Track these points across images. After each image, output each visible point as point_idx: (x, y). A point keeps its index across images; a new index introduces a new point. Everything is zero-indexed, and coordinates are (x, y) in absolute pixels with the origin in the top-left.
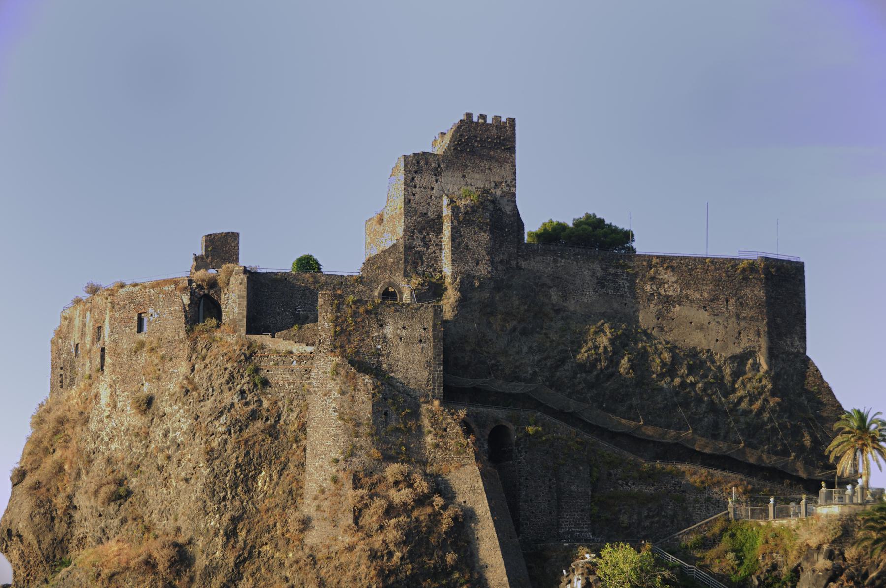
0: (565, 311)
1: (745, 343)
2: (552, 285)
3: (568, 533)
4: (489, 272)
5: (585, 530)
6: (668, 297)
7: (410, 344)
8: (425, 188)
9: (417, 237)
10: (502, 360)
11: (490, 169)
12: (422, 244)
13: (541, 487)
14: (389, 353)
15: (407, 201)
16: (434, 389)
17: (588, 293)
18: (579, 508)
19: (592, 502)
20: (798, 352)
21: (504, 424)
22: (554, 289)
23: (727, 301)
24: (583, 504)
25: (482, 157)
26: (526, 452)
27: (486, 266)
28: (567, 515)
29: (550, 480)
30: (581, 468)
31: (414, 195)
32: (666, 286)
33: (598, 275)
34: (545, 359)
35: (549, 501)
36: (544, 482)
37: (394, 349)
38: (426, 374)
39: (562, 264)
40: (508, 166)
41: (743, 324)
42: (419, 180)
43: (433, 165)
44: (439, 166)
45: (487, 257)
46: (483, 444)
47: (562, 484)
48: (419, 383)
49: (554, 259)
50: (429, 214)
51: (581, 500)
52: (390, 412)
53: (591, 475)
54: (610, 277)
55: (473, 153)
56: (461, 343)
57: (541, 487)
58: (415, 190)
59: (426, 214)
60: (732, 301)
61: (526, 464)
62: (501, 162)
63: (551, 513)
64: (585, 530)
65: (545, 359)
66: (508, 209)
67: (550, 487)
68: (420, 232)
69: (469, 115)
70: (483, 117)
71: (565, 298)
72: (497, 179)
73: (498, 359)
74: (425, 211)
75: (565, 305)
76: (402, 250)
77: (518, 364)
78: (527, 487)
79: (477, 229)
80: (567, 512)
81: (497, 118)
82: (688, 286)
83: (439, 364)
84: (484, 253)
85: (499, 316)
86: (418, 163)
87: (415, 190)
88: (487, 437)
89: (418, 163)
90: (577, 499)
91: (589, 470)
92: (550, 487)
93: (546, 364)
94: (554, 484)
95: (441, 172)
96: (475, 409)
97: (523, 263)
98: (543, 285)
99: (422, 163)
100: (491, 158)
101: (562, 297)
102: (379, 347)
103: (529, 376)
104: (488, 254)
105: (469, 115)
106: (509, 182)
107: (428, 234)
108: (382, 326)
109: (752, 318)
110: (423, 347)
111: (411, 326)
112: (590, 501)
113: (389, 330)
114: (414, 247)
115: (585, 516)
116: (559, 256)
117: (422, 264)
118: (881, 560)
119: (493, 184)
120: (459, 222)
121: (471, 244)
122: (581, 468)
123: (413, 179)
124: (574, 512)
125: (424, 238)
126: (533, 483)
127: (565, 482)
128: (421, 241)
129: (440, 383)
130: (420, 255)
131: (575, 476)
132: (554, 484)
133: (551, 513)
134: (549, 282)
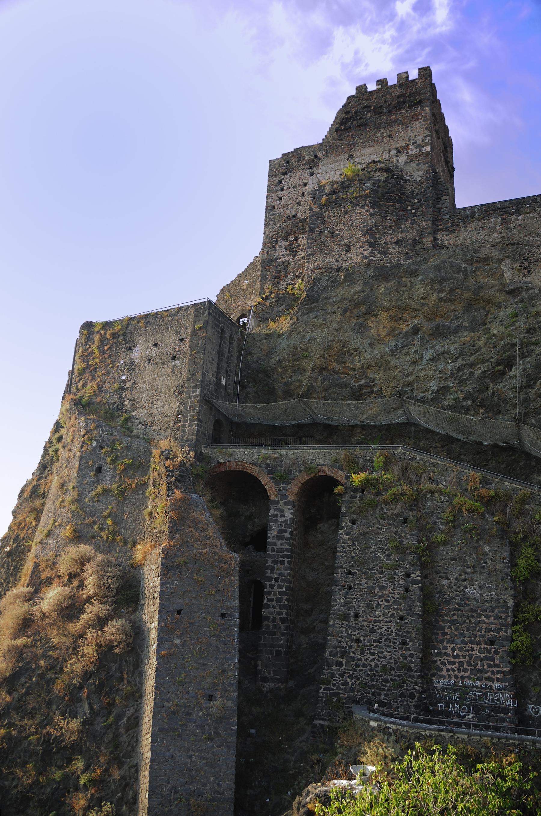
0: (527, 290)
2: (501, 257)
3: (455, 689)
4: (365, 258)
5: (496, 685)
7: (160, 365)
8: (294, 187)
9: (280, 246)
10: (378, 375)
11: (390, 136)
12: (288, 252)
13: (383, 588)
14: (134, 383)
15: (270, 209)
16: (184, 426)
18: (482, 636)
19: (514, 624)
21: (327, 474)
22: (508, 261)
24: (493, 627)
25: (378, 128)
26: (354, 522)
27: (361, 250)
28: (453, 650)
29: (408, 575)
30: (487, 549)
31: (280, 199)
34: (471, 365)
35: (401, 618)
36: (391, 579)
37: (140, 377)
38: (175, 405)
39: (519, 223)
42: (287, 181)
43: (307, 158)
44: (316, 156)
45: (363, 239)
46: (282, 511)
47: (445, 582)
48: (166, 419)
49: (503, 219)
50: (299, 215)
51: (487, 617)
52: (106, 467)
53: (513, 565)
56: (295, 360)
57: (383, 588)
58: (280, 194)
59: (294, 216)
61: (350, 543)
63: (404, 643)
64: (496, 685)
65: (471, 365)
67: (407, 590)
68: (286, 238)
70: (382, 82)
71: (527, 270)
72: (401, 144)
73: (371, 376)
74: (293, 213)
75: (528, 280)
76: (259, 267)
77: (410, 379)
78: (350, 588)
79: (349, 207)
80: (453, 642)
81: (403, 78)
83: (195, 387)
84: (360, 233)
85: (384, 315)
86: (288, 162)
87: (280, 194)
88: (291, 498)
89: (288, 162)
90: (480, 616)
91: (507, 554)
92: (407, 590)
93: (471, 374)
94: (414, 582)
95: (318, 163)
96: (270, 452)
97: (446, 238)
98: (486, 260)
99: (293, 160)
100: (390, 124)
101: (520, 270)
102: (124, 378)
103: (429, 395)
104: (364, 235)
107: (296, 239)
108: (130, 349)
110: (175, 366)
112: (510, 620)
114: (276, 259)
115: (496, 652)
116: (514, 213)
117: (286, 277)
119: (394, 152)
120: (321, 206)
122: (487, 549)
123: (280, 182)
124: (471, 642)
125: (291, 245)
126: (364, 581)
127: (452, 578)
128: (286, 249)
129: (193, 416)
130: (285, 266)
131: (474, 567)
132: (414, 582)
133: (404, 643)
134: (496, 254)
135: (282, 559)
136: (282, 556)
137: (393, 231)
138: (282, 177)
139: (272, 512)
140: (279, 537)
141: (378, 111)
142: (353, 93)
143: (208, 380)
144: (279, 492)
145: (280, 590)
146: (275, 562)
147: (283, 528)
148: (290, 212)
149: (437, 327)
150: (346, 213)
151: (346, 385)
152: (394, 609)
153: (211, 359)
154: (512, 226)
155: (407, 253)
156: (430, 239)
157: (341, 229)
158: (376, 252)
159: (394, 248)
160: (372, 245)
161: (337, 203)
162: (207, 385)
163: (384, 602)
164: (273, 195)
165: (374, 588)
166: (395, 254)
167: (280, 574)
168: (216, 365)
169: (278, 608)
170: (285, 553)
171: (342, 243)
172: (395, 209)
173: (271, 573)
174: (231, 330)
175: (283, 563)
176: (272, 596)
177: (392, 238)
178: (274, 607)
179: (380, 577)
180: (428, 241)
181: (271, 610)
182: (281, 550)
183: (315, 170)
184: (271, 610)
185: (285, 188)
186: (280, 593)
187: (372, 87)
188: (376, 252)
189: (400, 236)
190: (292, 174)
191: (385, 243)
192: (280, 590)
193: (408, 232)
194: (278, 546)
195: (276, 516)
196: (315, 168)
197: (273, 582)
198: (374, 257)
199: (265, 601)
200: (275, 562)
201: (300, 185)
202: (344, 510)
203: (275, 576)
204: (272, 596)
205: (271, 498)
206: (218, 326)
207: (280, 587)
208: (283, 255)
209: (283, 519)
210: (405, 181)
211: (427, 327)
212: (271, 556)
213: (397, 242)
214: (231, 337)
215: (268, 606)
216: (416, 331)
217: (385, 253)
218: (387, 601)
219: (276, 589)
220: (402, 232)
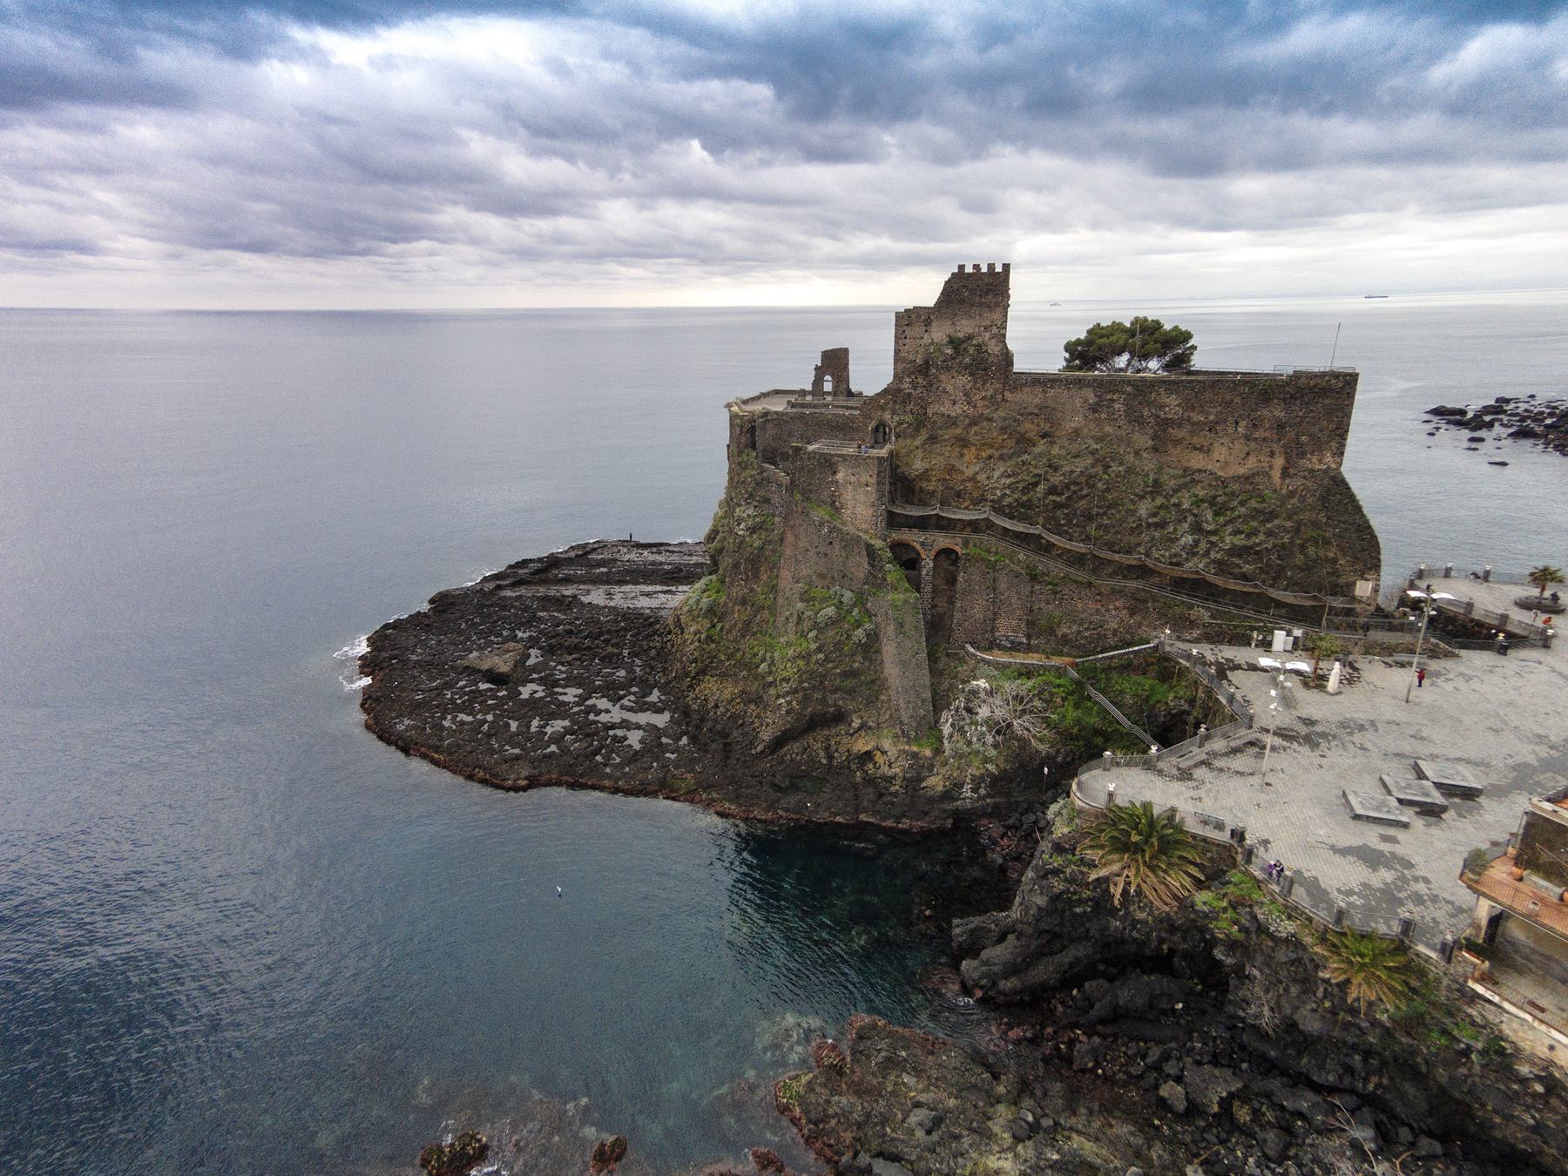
1: (1252, 463)
3: (1004, 636)
6: (1167, 419)
11: (980, 315)
15: (897, 352)
20: (1329, 468)
23: (1237, 423)
32: (1167, 409)
38: (870, 511)
40: (999, 310)
41: (1253, 445)
45: (964, 398)
54: (1105, 403)
55: (962, 301)
60: (1243, 423)
62: (991, 308)
65: (1017, 482)
66: (993, 348)
69: (962, 267)
72: (988, 323)
81: (991, 266)
82: (1193, 408)
99: (913, 316)
100: (981, 305)
105: (962, 267)
106: (999, 325)
109: (1265, 439)
111: (859, 474)
113: (840, 476)
118: (877, 994)
119: (982, 329)
121: (949, 388)
138: (905, 328)
141: (972, 291)
148: (911, 357)
149: (1001, 455)
150: (953, 377)
151: (952, 488)
156: (1001, 396)
160: (968, 403)
161: (949, 369)
180: (999, 397)
183: (928, 328)
187: (969, 269)
189: (984, 394)
210: (989, 354)
211: (996, 454)
213: (983, 398)
216: (990, 457)
217: (975, 407)
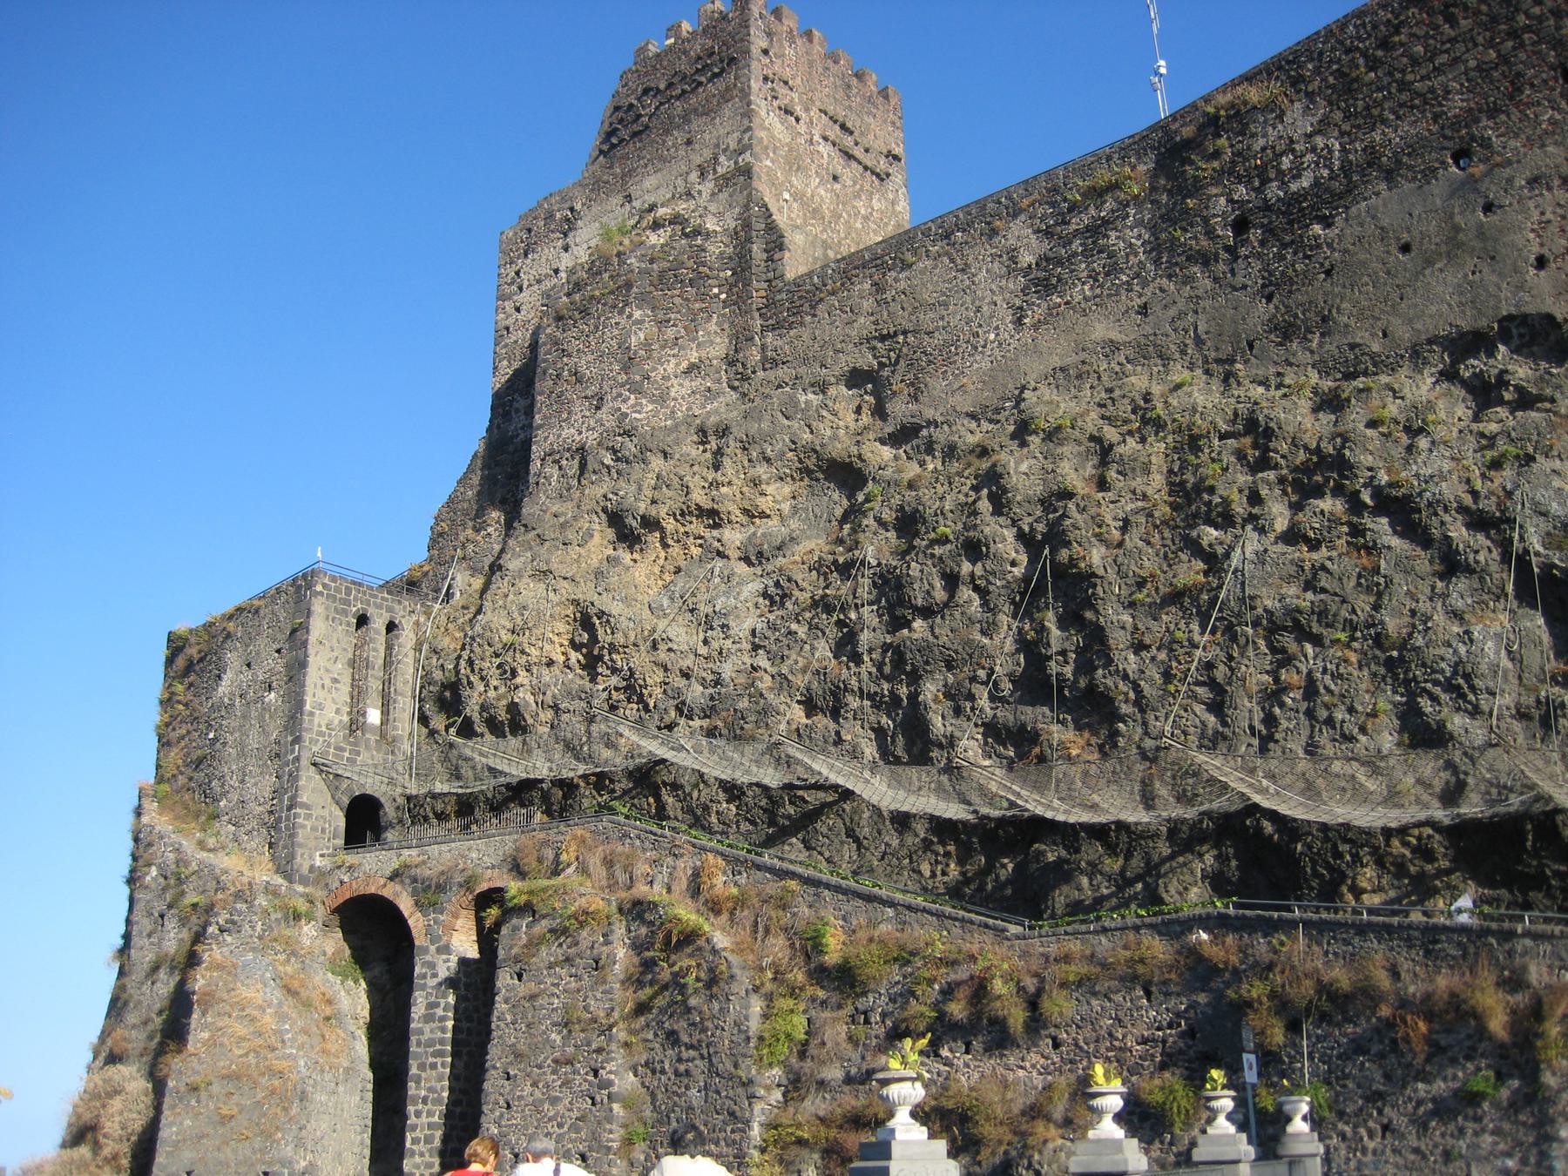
8: (539, 282)
9: (517, 411)
13: (554, 1101)
17: (992, 336)
31: (518, 310)
33: (1027, 258)
42: (531, 268)
108: (219, 677)
126: (528, 1089)
135: (431, 1060)
136: (435, 1055)
137: (682, 348)
139: (418, 970)
140: (428, 1018)
142: (629, 63)
143: (323, 723)
144: (428, 931)
145: (430, 1119)
146: (422, 1067)
147: (433, 999)
152: (571, 1141)
153: (327, 682)
154: (888, 295)
155: (709, 390)
157: (584, 364)
158: (644, 401)
159: (681, 385)
162: (321, 734)
163: (556, 1128)
164: (506, 303)
165: (542, 1102)
166: (683, 398)
167: (430, 1090)
168: (345, 688)
169: (427, 1155)
170: (438, 1047)
171: (589, 393)
172: (687, 299)
173: (417, 1089)
174: (389, 610)
175: (433, 1066)
176: (418, 1133)
177: (677, 365)
178: (422, 1155)
179: (554, 1081)
181: (417, 1159)
182: (430, 1043)
184: (417, 1159)
185: (525, 287)
186: (430, 1126)
188: (644, 401)
189: (694, 356)
190: (536, 256)
191: (663, 378)
192: (430, 1119)
193: (712, 343)
194: (427, 1036)
195: (424, 976)
196: (571, 235)
197: (420, 1106)
198: (639, 412)
199: (408, 1144)
200: (422, 1067)
201: (547, 276)
202: (501, 953)
203: (423, 1093)
204: (418, 1133)
205: (417, 943)
206: (345, 613)
207: (430, 1114)
208: (522, 428)
209: (435, 981)
212: (418, 1056)
213: (692, 369)
214: (391, 627)
215: (413, 1153)
217: (662, 399)
218: (560, 1126)
219: (424, 1119)
220: (699, 345)
